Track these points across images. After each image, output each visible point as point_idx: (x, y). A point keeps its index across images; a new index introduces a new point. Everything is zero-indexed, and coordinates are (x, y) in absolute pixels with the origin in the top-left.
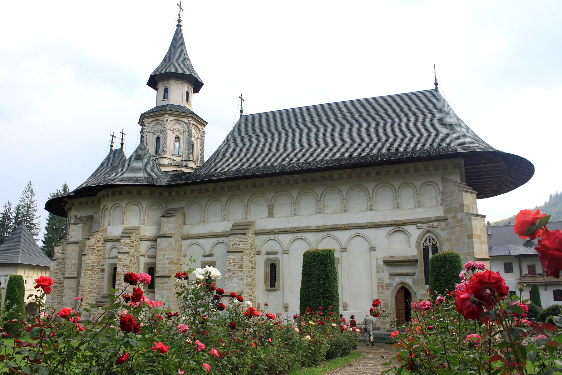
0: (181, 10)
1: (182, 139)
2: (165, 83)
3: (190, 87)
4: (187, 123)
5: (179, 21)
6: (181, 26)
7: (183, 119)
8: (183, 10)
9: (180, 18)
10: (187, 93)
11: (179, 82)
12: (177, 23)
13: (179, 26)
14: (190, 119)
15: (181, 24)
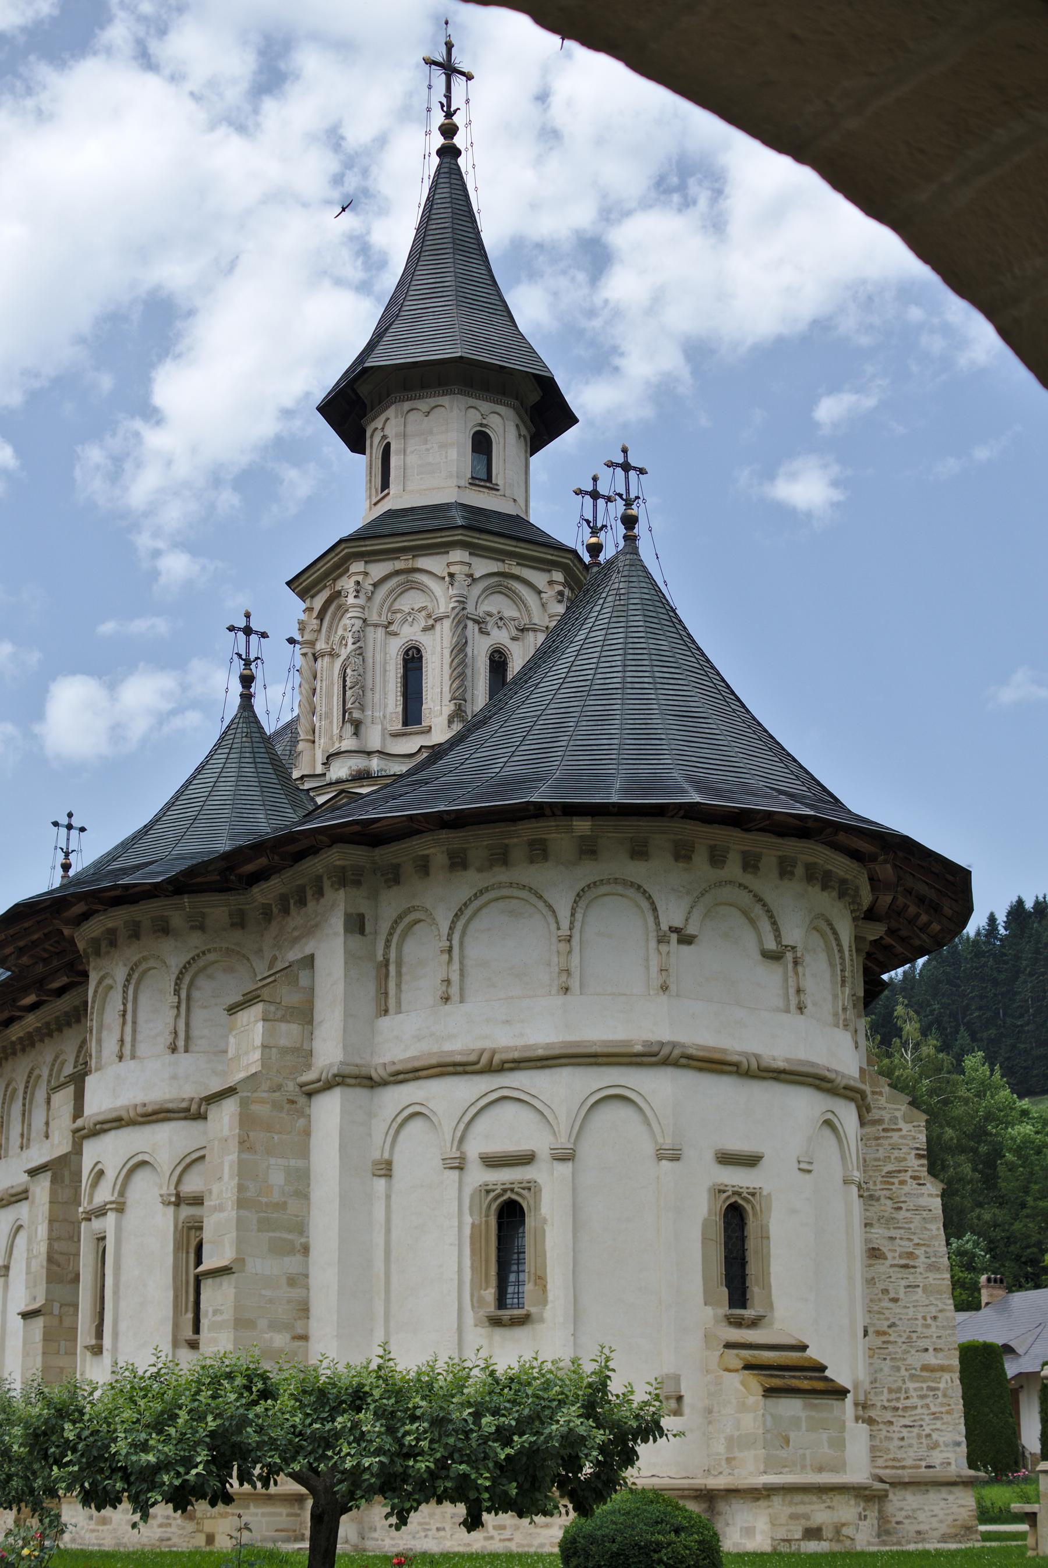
0: (458, 82)
1: (429, 650)
2: (378, 423)
3: (485, 406)
4: (444, 578)
5: (449, 131)
6: (457, 153)
7: (423, 563)
8: (469, 77)
9: (449, 115)
10: (482, 444)
11: (423, 405)
12: (438, 140)
13: (449, 153)
14: (458, 555)
15: (458, 141)
